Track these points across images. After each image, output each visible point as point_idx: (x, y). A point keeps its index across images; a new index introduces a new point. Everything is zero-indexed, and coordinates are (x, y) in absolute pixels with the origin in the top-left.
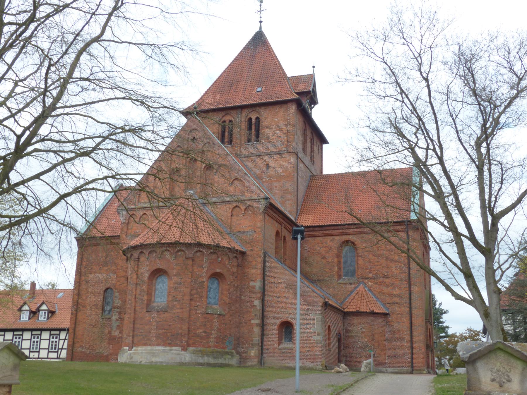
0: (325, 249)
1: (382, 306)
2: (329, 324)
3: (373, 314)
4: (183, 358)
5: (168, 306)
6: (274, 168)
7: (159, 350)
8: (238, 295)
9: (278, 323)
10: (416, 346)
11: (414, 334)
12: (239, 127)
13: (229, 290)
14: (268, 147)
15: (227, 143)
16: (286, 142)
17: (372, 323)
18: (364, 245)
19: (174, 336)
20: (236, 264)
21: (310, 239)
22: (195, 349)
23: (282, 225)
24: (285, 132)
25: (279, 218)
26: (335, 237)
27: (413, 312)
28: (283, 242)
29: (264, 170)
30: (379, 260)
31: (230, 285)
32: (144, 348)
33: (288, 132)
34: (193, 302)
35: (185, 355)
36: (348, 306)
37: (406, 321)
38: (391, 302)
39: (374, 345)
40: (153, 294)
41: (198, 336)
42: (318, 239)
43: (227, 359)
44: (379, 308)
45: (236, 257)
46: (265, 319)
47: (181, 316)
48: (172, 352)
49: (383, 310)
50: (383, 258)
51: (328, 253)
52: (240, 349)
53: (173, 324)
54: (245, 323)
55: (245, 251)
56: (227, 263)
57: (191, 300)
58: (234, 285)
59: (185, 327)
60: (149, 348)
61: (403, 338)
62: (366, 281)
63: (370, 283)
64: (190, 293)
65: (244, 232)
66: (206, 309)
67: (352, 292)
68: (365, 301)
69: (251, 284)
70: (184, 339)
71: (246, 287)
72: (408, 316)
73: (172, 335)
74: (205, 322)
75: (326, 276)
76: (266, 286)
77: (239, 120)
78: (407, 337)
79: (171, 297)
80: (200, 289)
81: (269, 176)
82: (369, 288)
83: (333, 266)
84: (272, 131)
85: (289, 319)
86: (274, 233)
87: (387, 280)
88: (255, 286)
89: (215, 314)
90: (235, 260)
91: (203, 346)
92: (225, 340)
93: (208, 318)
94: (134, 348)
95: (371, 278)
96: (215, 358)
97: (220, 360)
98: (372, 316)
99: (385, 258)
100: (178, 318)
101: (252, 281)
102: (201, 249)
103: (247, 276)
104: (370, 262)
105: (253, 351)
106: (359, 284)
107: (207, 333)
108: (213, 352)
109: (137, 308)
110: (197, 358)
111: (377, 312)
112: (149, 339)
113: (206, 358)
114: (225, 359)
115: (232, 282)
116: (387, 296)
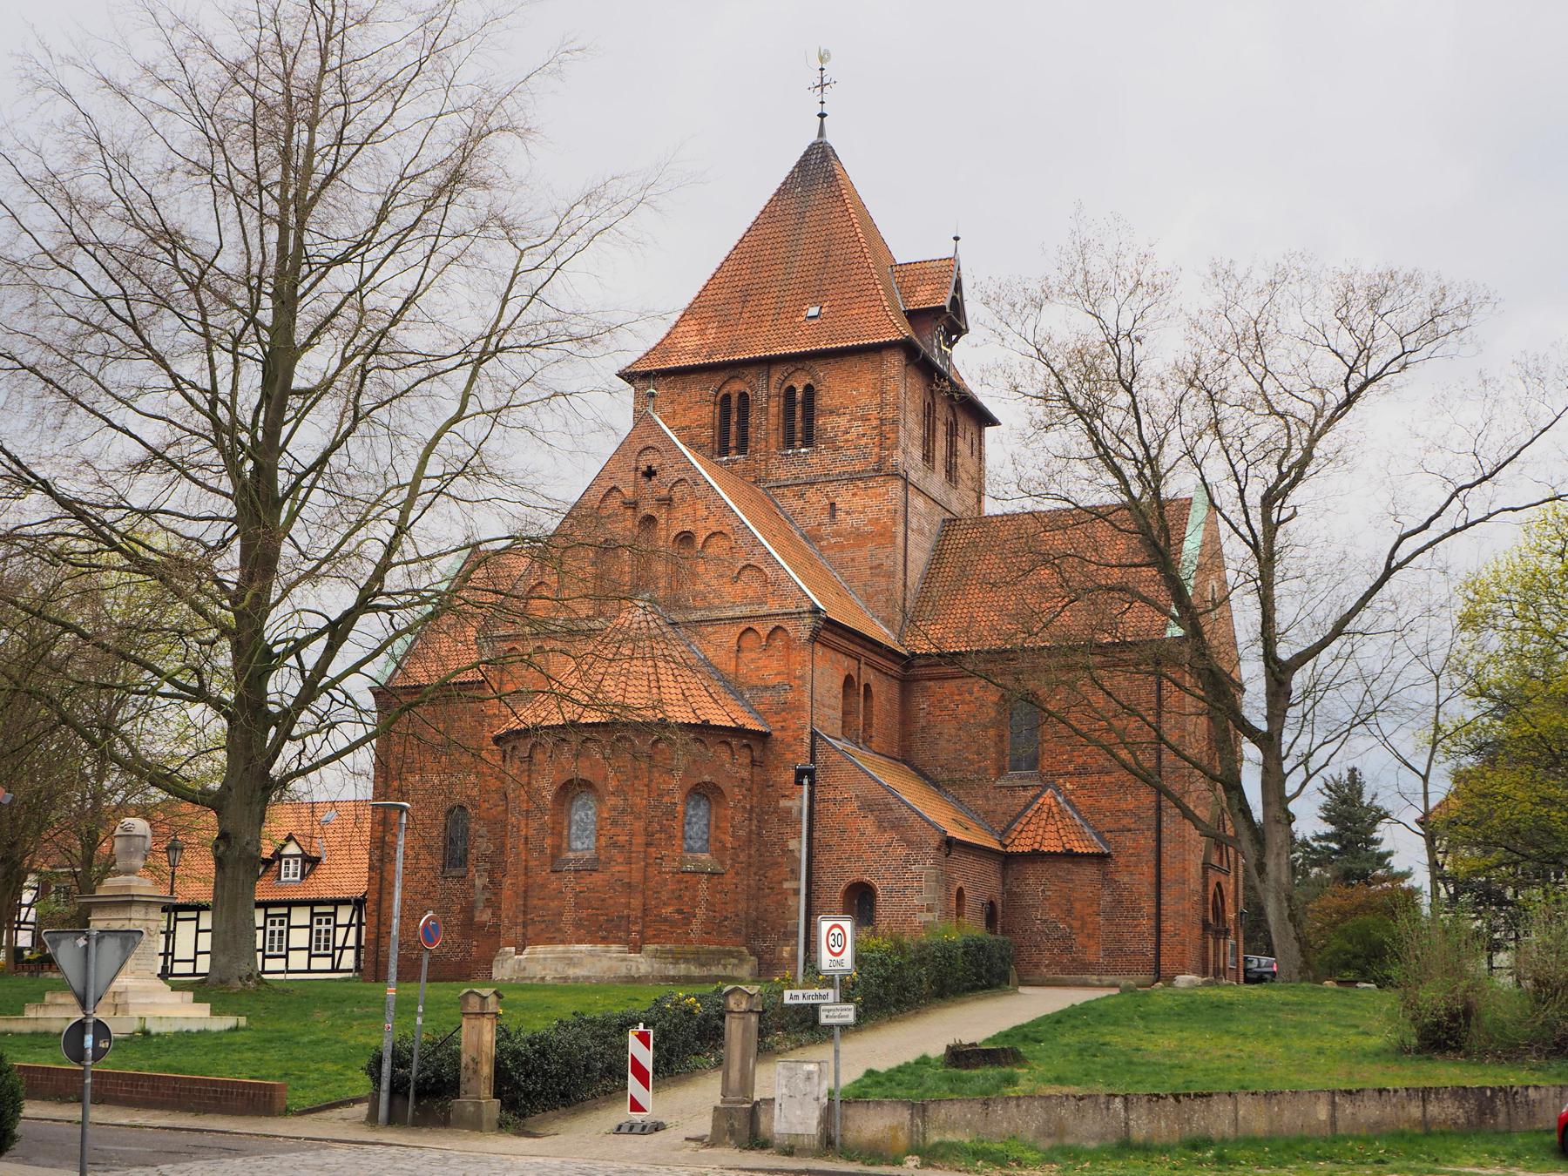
2: (959, 884)
3: (1070, 856)
4: (634, 969)
5: (597, 859)
6: (847, 513)
9: (843, 887)
10: (1167, 925)
11: (1165, 898)
12: (765, 411)
13: (733, 818)
14: (834, 461)
15: (734, 452)
16: (877, 450)
20: (748, 761)
21: (932, 683)
23: (859, 661)
24: (875, 423)
25: (851, 646)
27: (1163, 850)
28: (862, 700)
29: (825, 518)
31: (735, 807)
32: (549, 948)
33: (882, 424)
37: (1148, 870)
38: (1115, 826)
39: (1071, 927)
40: (565, 833)
41: (665, 920)
42: (951, 685)
45: (747, 746)
46: (815, 878)
47: (626, 880)
49: (1096, 847)
52: (760, 945)
57: (648, 845)
59: (636, 902)
60: (560, 948)
61: (1140, 910)
63: (1068, 785)
65: (767, 688)
66: (682, 863)
67: (1027, 807)
68: (1054, 828)
69: (783, 803)
72: (1152, 856)
76: (816, 806)
77: (762, 393)
78: (1148, 907)
79: (603, 839)
81: (837, 534)
82: (1065, 796)
84: (843, 421)
85: (866, 878)
86: (840, 681)
87: (1107, 779)
88: (791, 808)
90: (746, 751)
91: (677, 941)
94: (527, 950)
96: (702, 965)
105: (788, 948)
106: (1044, 787)
109: (532, 863)
112: (559, 930)
114: (725, 967)
115: (739, 801)
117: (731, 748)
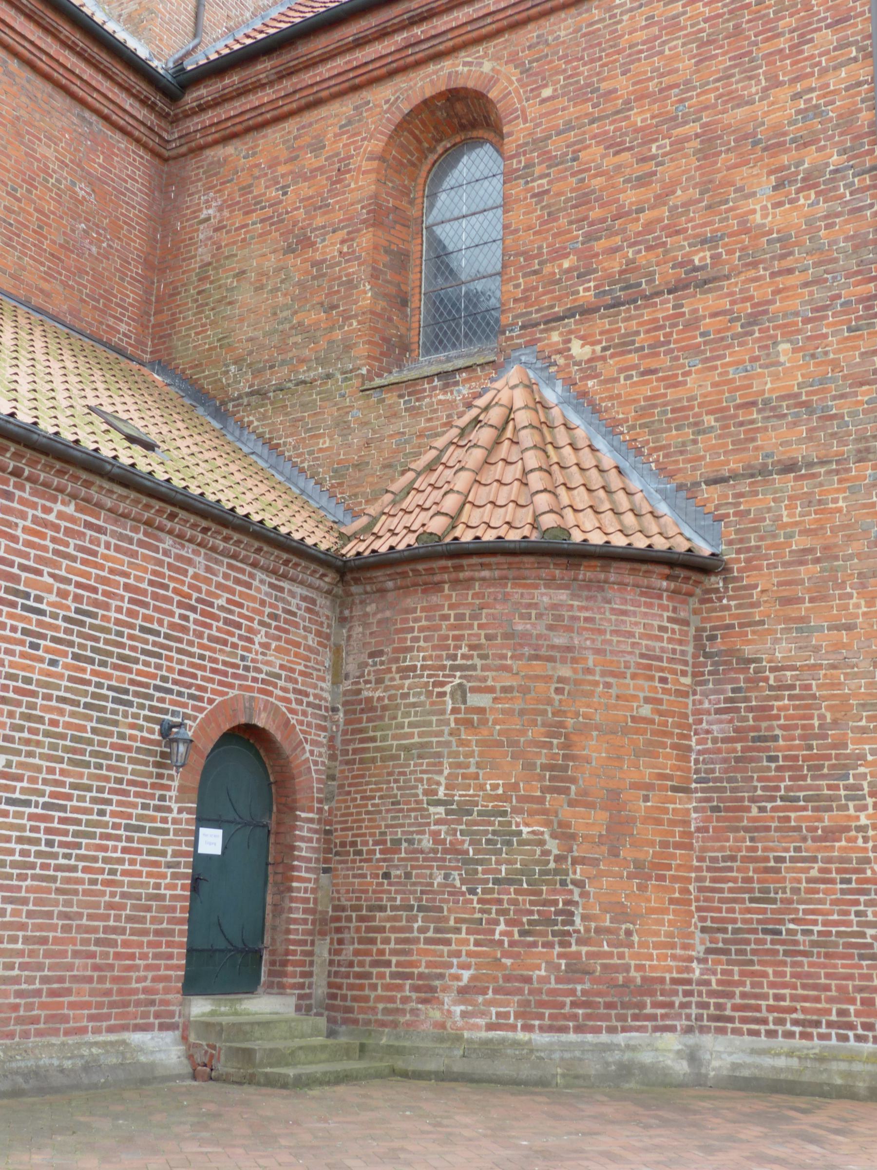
0: (305, 189)
1: (663, 508)
17: (559, 640)
18: (547, 92)
26: (366, 95)
30: (651, 166)
36: (374, 520)
38: (734, 464)
39: (564, 833)
44: (629, 519)
50: (679, 143)
51: (324, 207)
61: (842, 769)
62: (555, 337)
63: (578, 350)
75: (302, 361)
82: (570, 383)
83: (350, 284)
95: (587, 311)
98: (551, 582)
99: (696, 144)
104: (584, 199)
111: (597, 539)
116: (709, 420)
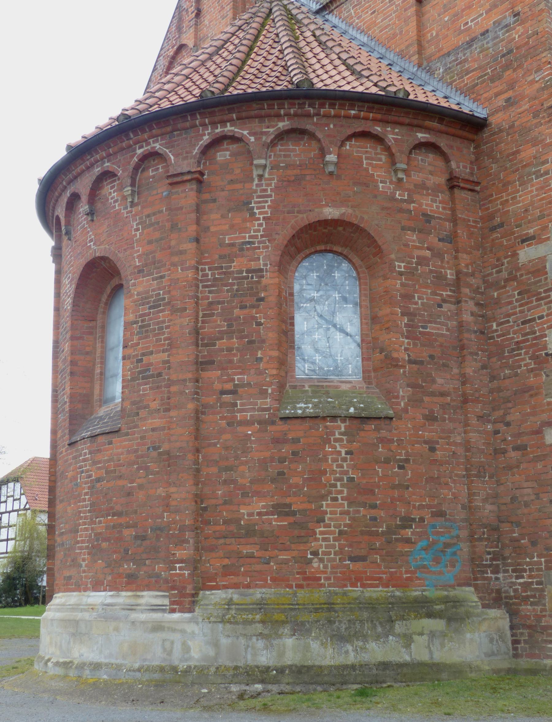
4: (178, 647)
7: (92, 608)
8: (467, 317)
13: (407, 297)
19: (143, 538)
20: (441, 180)
22: (236, 597)
31: (410, 273)
34: (212, 374)
35: (183, 631)
43: (421, 641)
47: (165, 447)
48: (134, 616)
53: (141, 487)
54: (516, 448)
55: (481, 112)
56: (378, 174)
58: (440, 277)
64: (197, 332)
70: (179, 553)
71: (505, 274)
73: (136, 537)
74: (282, 460)
80: (243, 307)
89: (334, 418)
91: (278, 580)
92: (408, 541)
93: (296, 441)
97: (372, 645)
100: (154, 454)
101: (526, 240)
102: (229, 128)
103: (501, 225)
107: (294, 513)
108: (330, 607)
110: (242, 641)
113: (290, 642)
115: (422, 261)
117: (388, 149)
